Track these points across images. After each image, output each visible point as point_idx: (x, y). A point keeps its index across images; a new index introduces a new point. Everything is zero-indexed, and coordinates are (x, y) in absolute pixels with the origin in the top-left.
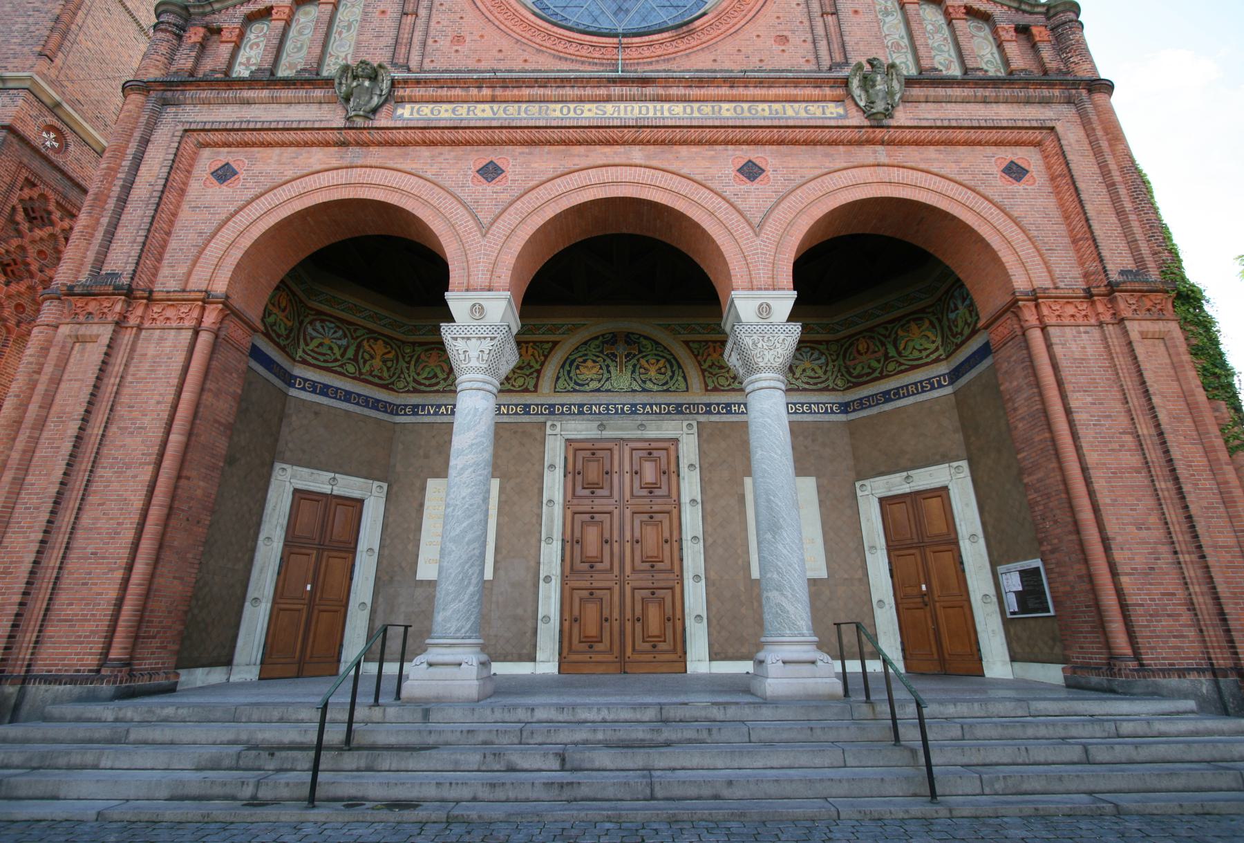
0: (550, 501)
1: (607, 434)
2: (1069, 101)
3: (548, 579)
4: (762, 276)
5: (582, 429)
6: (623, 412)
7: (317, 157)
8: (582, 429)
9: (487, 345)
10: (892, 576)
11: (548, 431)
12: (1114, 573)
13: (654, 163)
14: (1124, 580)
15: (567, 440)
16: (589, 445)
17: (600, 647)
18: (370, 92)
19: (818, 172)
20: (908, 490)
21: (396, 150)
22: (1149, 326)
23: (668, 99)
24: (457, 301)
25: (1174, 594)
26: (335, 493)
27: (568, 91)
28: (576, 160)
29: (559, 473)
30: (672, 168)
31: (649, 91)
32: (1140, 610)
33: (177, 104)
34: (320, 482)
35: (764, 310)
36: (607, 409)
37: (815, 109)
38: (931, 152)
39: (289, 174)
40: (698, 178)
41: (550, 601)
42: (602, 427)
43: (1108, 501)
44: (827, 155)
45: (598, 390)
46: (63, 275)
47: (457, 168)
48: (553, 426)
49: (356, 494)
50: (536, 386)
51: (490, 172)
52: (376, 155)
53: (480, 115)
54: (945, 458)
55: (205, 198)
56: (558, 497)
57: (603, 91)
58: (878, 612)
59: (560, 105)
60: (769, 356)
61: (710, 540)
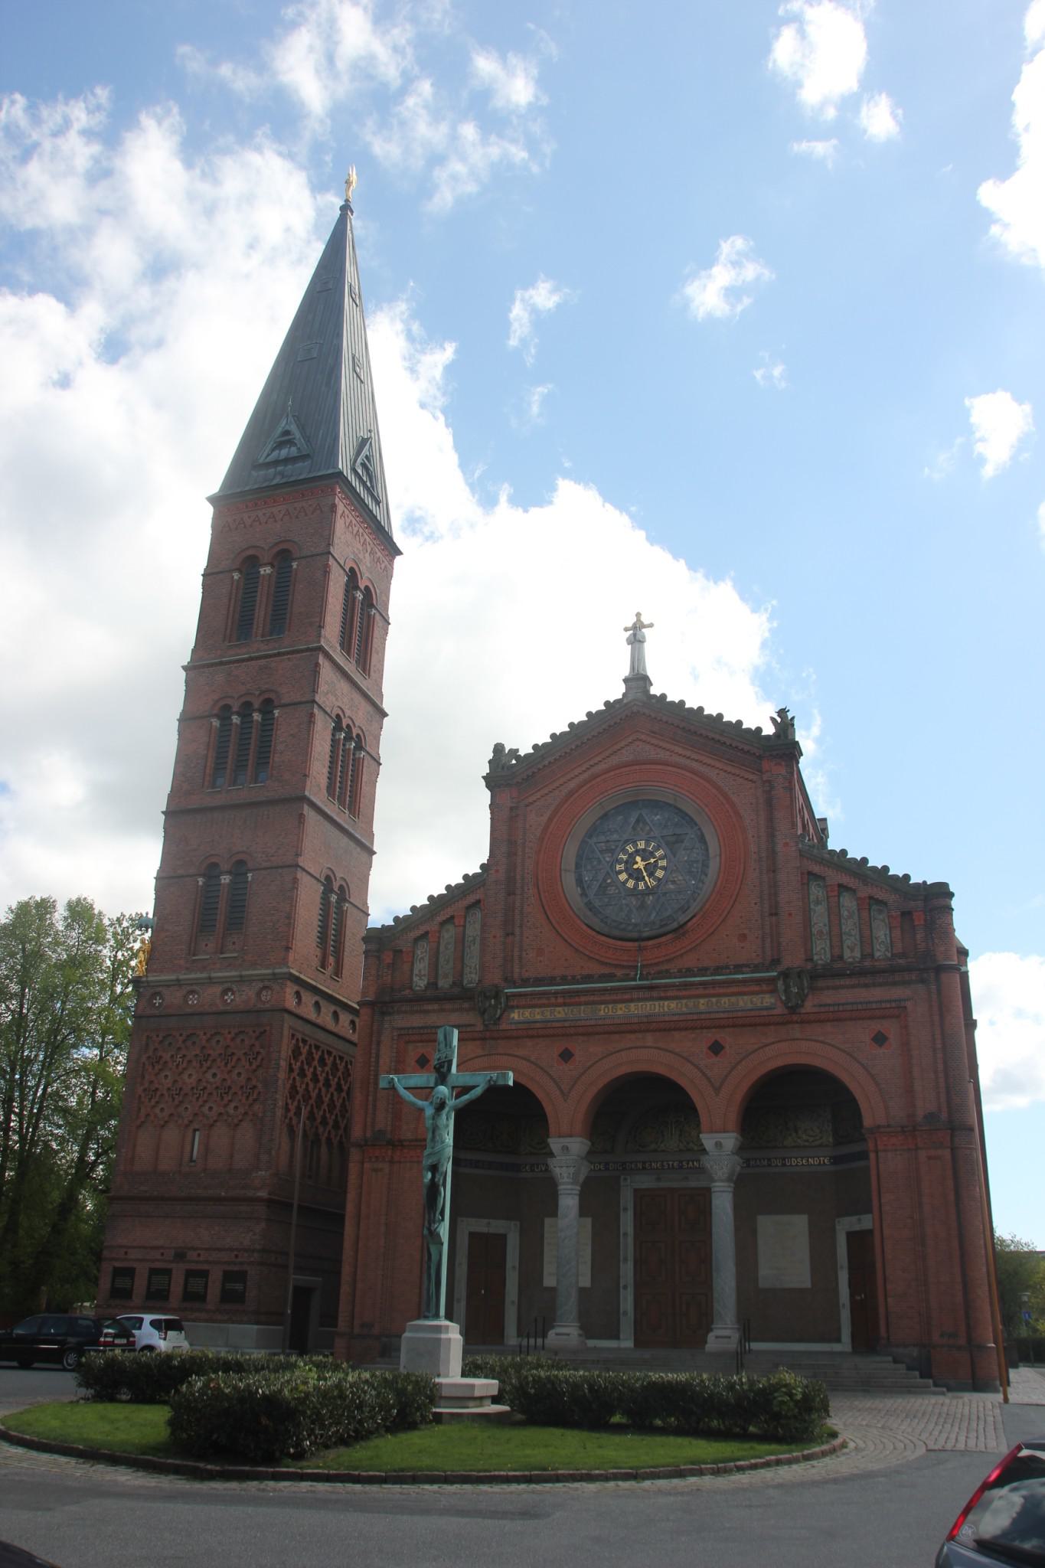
2: (923, 981)
9: (572, 1170)
23: (667, 998)
24: (555, 1144)
27: (607, 997)
33: (390, 1014)
35: (719, 1145)
37: (756, 999)
53: (559, 1016)
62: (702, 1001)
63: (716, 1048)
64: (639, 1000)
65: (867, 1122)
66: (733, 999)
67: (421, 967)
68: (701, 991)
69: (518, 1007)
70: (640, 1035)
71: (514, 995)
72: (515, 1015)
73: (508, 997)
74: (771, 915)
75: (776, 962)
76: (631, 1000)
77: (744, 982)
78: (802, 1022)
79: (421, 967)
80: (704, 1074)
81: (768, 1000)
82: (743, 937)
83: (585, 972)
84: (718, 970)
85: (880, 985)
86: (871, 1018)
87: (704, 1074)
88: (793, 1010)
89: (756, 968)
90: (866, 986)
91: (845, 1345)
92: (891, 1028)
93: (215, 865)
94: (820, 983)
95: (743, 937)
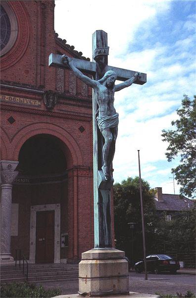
12: (78, 238)
14: (80, 239)
19: (30, 123)
25: (88, 242)
37: (33, 102)
44: (34, 118)
54: (55, 202)
58: (31, 246)
60: (9, 180)
62: (7, 97)
66: (22, 99)
74: (41, 65)
75: (42, 87)
77: (28, 92)
78: (52, 116)
81: (38, 103)
82: (27, 72)
84: (14, 84)
85: (84, 107)
86: (80, 120)
88: (49, 110)
89: (32, 87)
90: (79, 106)
95: (27, 72)
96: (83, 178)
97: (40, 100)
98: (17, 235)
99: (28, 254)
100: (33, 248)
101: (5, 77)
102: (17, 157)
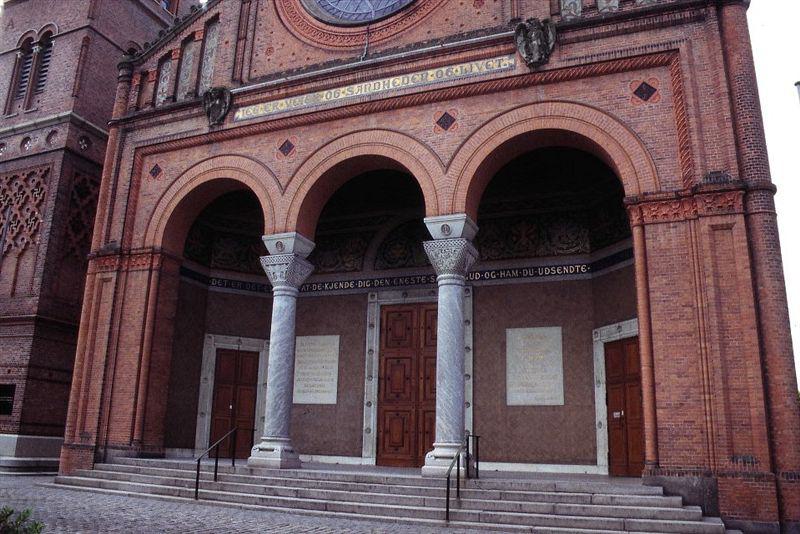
0: (370, 350)
1: (409, 300)
3: (369, 404)
4: (445, 205)
5: (392, 298)
6: (420, 282)
7: (197, 154)
8: (392, 298)
10: (607, 404)
11: (370, 300)
13: (384, 125)
14: (660, 412)
15: (381, 306)
16: (396, 309)
17: (403, 449)
18: (220, 106)
19: (493, 115)
20: (618, 338)
21: (236, 141)
22: (719, 221)
23: (392, 74)
26: (241, 349)
28: (336, 131)
29: (376, 330)
30: (393, 128)
31: (379, 71)
32: (665, 432)
34: (231, 343)
35: (446, 229)
36: (410, 280)
37: (493, 63)
38: (580, 85)
39: (185, 167)
40: (411, 132)
41: (370, 419)
42: (405, 295)
43: (661, 357)
45: (403, 266)
46: (96, 243)
47: (267, 148)
48: (373, 296)
49: (254, 349)
50: (362, 266)
51: (287, 148)
52: (226, 147)
53: (282, 108)
55: (150, 186)
56: (376, 347)
57: (351, 78)
59: (325, 92)
60: (446, 262)
61: (478, 377)
62: (430, 72)
63: (446, 122)
64: (362, 80)
65: (630, 190)
66: (466, 66)
67: (165, 85)
68: (429, 61)
69: (243, 105)
70: (362, 118)
71: (239, 94)
72: (240, 114)
73: (233, 96)
76: (354, 82)
78: (547, 82)
79: (165, 85)
80: (431, 151)
83: (310, 63)
85: (643, 29)
86: (633, 69)
87: (431, 151)
88: (536, 67)
90: (626, 32)
91: (602, 468)
92: (660, 79)
93: (31, 39)
94: (570, 35)
96: (661, 228)
97: (511, 53)
98: (561, 402)
99: (595, 450)
100: (602, 436)
101: (429, 32)
102: (461, 204)
